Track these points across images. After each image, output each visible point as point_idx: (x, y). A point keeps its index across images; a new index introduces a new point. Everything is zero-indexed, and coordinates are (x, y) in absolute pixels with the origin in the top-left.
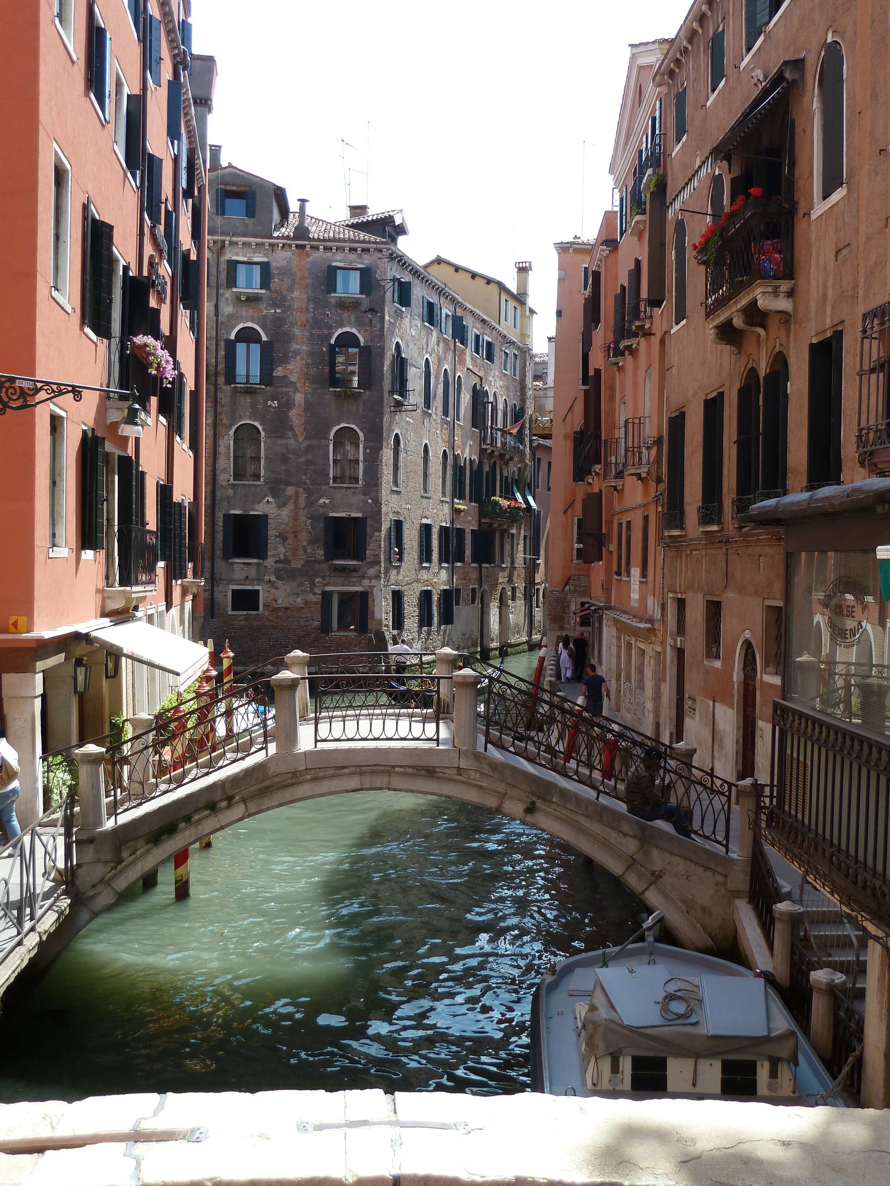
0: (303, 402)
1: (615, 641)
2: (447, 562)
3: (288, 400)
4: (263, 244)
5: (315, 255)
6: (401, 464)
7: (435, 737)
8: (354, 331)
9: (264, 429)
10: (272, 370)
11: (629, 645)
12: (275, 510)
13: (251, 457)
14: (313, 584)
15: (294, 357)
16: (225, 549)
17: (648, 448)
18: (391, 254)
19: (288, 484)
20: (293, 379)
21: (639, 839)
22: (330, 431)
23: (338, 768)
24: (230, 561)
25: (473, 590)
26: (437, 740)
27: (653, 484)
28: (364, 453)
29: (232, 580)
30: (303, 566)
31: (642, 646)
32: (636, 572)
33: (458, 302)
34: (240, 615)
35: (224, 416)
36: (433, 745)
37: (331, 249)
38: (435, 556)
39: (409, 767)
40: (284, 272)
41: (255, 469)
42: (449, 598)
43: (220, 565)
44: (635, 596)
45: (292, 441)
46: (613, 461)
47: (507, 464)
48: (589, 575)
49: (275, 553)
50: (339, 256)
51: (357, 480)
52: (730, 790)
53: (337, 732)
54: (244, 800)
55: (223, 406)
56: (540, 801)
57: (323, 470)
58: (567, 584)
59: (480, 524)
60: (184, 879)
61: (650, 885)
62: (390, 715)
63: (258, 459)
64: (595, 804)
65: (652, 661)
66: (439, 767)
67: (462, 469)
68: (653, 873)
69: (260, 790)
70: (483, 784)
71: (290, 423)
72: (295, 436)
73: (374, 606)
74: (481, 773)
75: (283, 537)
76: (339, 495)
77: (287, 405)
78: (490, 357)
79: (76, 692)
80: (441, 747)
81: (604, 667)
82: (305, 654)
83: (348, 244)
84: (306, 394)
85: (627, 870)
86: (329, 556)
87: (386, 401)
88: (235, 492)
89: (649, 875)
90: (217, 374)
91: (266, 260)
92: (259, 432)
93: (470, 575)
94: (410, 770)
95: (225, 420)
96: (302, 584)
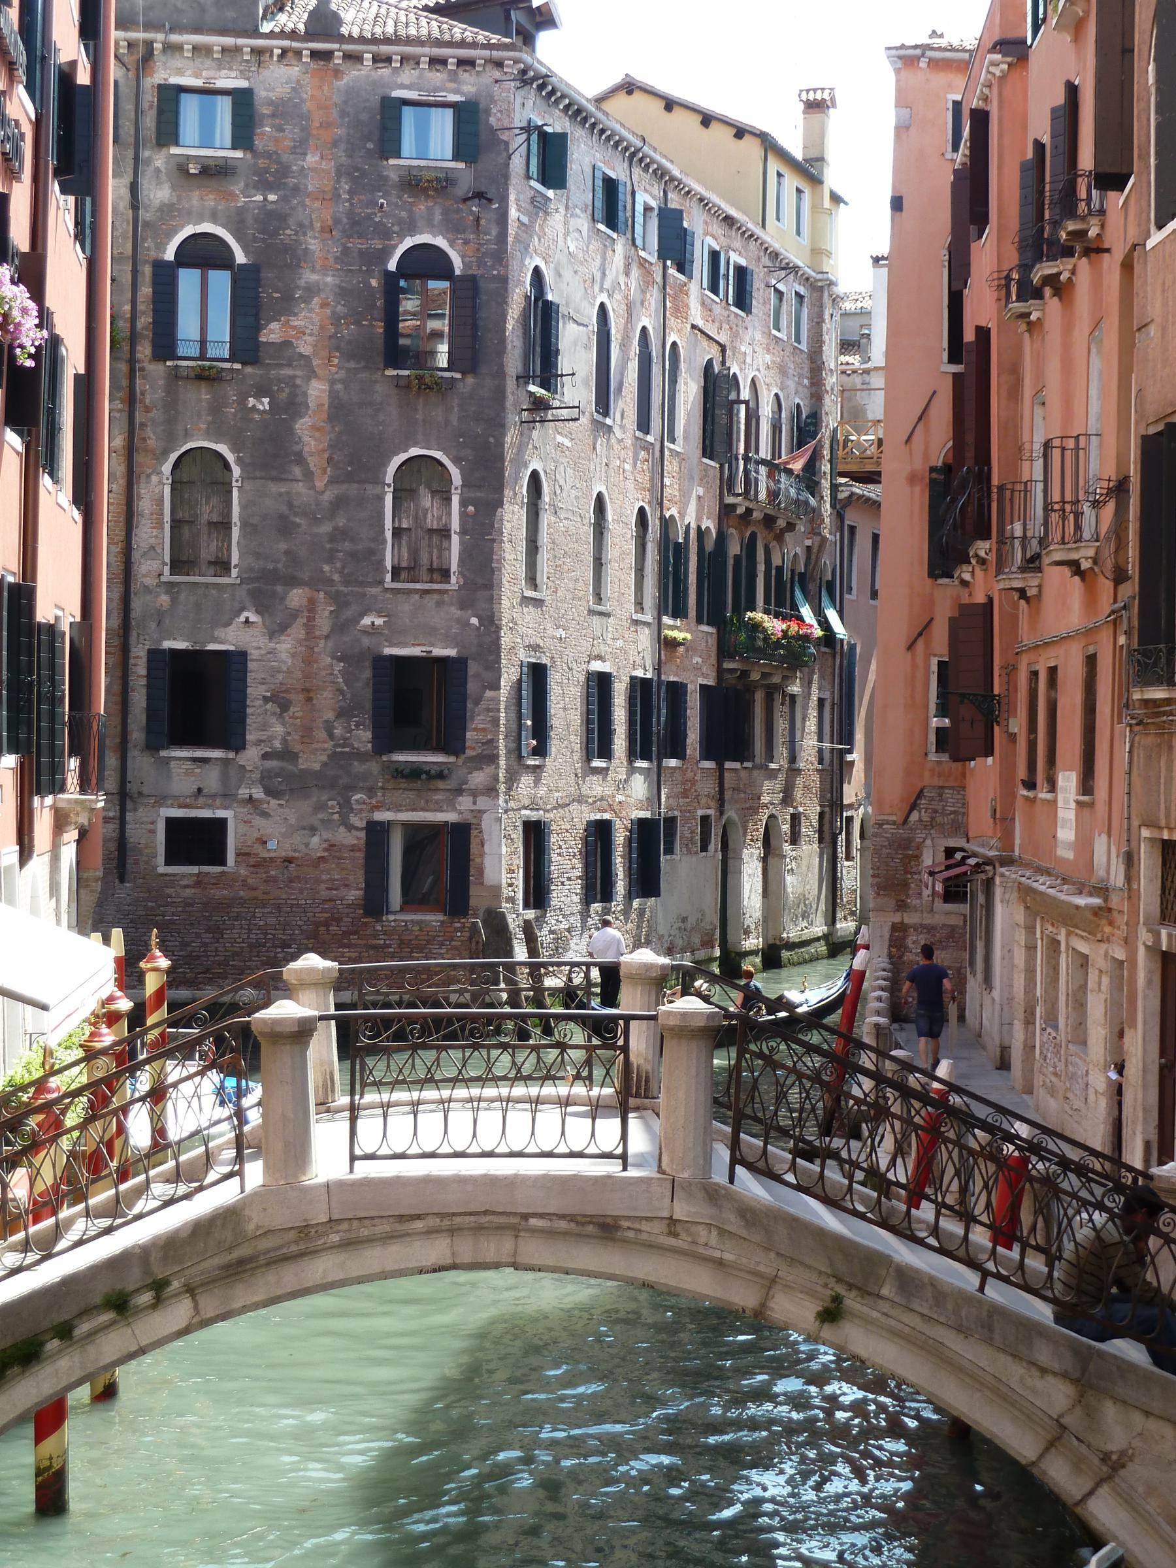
0: (325, 400)
1: (1021, 936)
2: (646, 756)
3: (293, 395)
4: (238, 49)
5: (353, 74)
6: (544, 538)
7: (619, 1151)
8: (440, 242)
9: (239, 461)
10: (258, 328)
11: (1054, 944)
12: (263, 641)
13: (210, 524)
14: (346, 807)
15: (307, 300)
16: (150, 729)
17: (1096, 504)
18: (524, 72)
19: (292, 582)
20: (305, 347)
21: (1076, 1382)
22: (385, 463)
23: (401, 1218)
24: (163, 753)
25: (705, 819)
26: (624, 1157)
27: (1105, 585)
28: (463, 515)
29: (165, 797)
30: (324, 765)
31: (1083, 947)
32: (1068, 781)
33: (672, 179)
34: (184, 876)
35: (149, 432)
36: (613, 1168)
37: (388, 60)
38: (620, 743)
39: (562, 1217)
40: (284, 110)
41: (220, 549)
42: (650, 838)
43: (140, 762)
44: (1066, 834)
45: (300, 487)
46: (1018, 532)
47: (779, 538)
48: (964, 788)
49: (263, 736)
50: (408, 75)
51: (445, 574)
53: (399, 1139)
54: (190, 1290)
55: (147, 410)
56: (854, 1294)
57: (371, 552)
58: (913, 807)
59: (720, 672)
60: (56, 1466)
61: (1098, 1485)
62: (518, 1101)
63: (226, 526)
64: (974, 1301)
65: (1106, 980)
66: (628, 1218)
67: (680, 550)
68: (1105, 1457)
69: (227, 1267)
70: (727, 1256)
71: (297, 448)
72: (308, 475)
73: (482, 855)
74: (722, 1232)
75: (280, 701)
76: (405, 607)
77: (292, 406)
78: (743, 300)
80: (632, 1173)
81: (996, 994)
82: (329, 964)
83: (427, 50)
84: (332, 383)
85: (1047, 1449)
86: (385, 743)
87: (510, 399)
88: (174, 600)
89: (1096, 1461)
90: (134, 338)
91: (242, 84)
92: (226, 466)
93: (699, 786)
94: (563, 1225)
95: (152, 438)
96: (321, 807)
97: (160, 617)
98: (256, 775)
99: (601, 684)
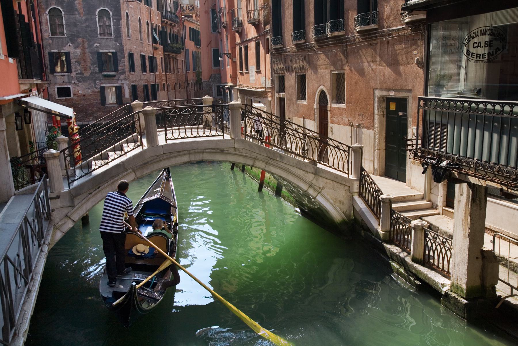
6: (130, 27)
9: (63, 11)
12: (73, 50)
13: (59, 24)
19: (78, 37)
25: (164, 84)
28: (113, 22)
38: (148, 69)
39: (212, 149)
45: (78, 16)
47: (173, 28)
51: (111, 35)
52: (349, 150)
53: (176, 135)
59: (164, 55)
63: (63, 25)
68: (320, 188)
72: (79, 13)
75: (78, 62)
76: (103, 41)
79: (17, 130)
86: (101, 70)
88: (52, 41)
95: (43, 6)
96: (90, 84)
97: (50, 45)
98: (75, 78)
99: (143, 57)
